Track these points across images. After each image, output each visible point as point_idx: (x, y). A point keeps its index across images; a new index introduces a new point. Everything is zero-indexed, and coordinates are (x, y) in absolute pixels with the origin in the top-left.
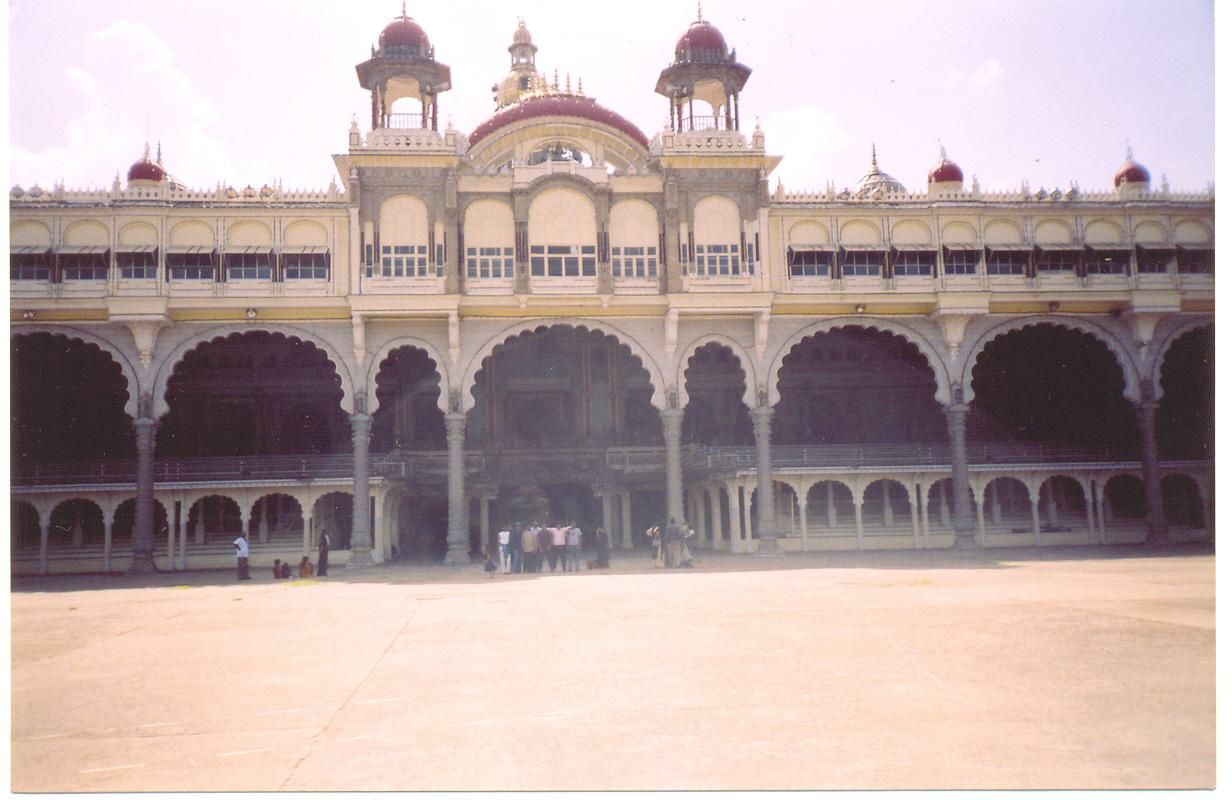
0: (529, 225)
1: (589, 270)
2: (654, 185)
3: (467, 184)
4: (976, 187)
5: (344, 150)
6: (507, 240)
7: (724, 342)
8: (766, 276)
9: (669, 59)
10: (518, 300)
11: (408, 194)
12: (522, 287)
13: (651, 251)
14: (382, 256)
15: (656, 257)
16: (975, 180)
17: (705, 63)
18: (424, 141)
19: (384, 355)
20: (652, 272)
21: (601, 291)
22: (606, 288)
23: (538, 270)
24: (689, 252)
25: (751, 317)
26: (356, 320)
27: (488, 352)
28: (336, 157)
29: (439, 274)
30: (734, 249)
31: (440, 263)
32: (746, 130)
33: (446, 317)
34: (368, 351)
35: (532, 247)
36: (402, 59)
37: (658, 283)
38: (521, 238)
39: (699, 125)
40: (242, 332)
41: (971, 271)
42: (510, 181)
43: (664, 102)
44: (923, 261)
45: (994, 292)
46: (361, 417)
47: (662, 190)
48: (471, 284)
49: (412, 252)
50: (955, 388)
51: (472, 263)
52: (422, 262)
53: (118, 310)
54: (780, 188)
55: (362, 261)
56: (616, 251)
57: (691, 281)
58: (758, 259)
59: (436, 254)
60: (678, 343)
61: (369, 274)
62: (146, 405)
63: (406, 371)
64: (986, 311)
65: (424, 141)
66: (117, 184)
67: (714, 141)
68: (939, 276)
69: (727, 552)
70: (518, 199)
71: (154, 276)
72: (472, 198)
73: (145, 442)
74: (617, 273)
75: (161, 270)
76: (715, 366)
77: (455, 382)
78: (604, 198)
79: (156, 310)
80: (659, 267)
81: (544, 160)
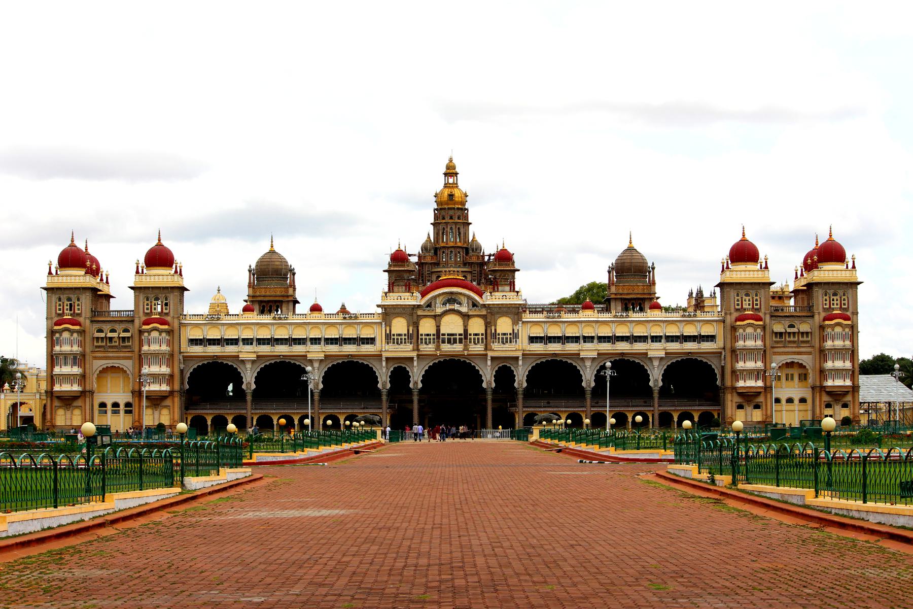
1: (461, 342)
2: (484, 312)
3: (420, 313)
5: (379, 303)
6: (433, 331)
22: (466, 348)
23: (443, 342)
24: (495, 335)
38: (438, 331)
41: (592, 342)
44: (576, 339)
53: (310, 356)
57: (496, 346)
59: (409, 336)
63: (400, 375)
75: (322, 342)
76: (505, 374)
77: (416, 379)
78: (466, 317)
79: (322, 356)
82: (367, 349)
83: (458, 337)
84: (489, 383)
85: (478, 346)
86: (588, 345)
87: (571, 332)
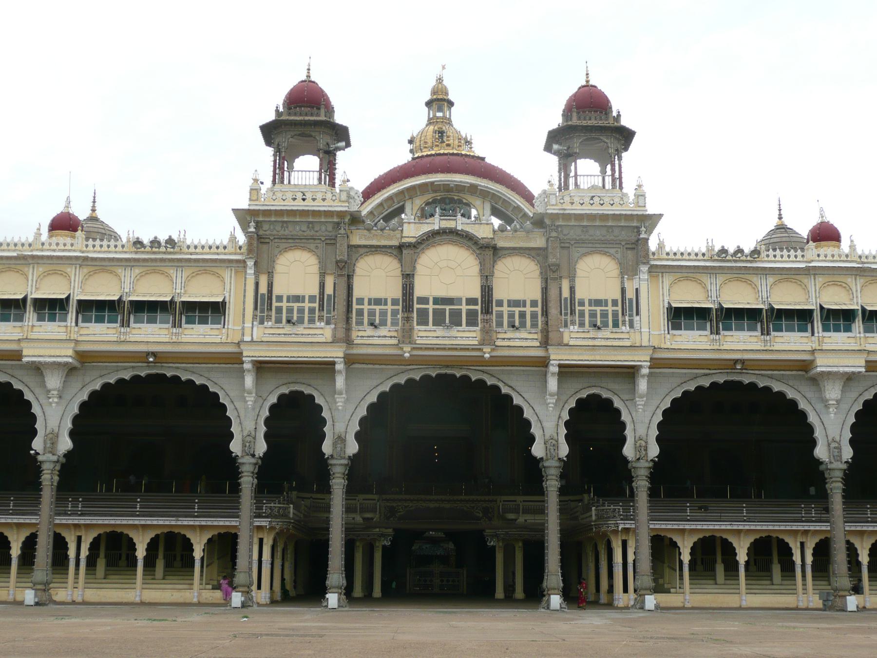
0: (416, 277)
1: (472, 320)
2: (539, 241)
3: (358, 238)
4: (852, 247)
5: (244, 204)
6: (393, 290)
7: (605, 395)
8: (645, 330)
9: (556, 121)
10: (402, 349)
11: (303, 248)
12: (407, 335)
13: (534, 303)
14: (275, 304)
15: (539, 309)
16: (852, 241)
17: (591, 126)
18: (319, 196)
19: (273, 399)
20: (534, 325)
21: (483, 342)
22: (487, 338)
23: (423, 321)
24: (571, 304)
25: (632, 370)
26: (247, 366)
27: (373, 398)
28: (235, 211)
29: (328, 323)
30: (615, 303)
31: (329, 312)
32: (629, 188)
33: (333, 364)
34: (258, 396)
35: (418, 298)
36: (305, 123)
37: (540, 335)
39: (584, 183)
40: (143, 374)
41: (848, 329)
42: (399, 236)
43: (553, 161)
45: (869, 352)
46: (248, 459)
47: (545, 246)
48: (354, 334)
49: (303, 302)
50: (833, 445)
51: (360, 313)
52: (312, 311)
53: (30, 354)
54: (661, 246)
55: (256, 308)
56: (500, 303)
57: (572, 334)
58: (637, 314)
60: (559, 393)
61: (262, 322)
62: (53, 439)
63: (295, 419)
64: (863, 370)
65: (319, 196)
66: (38, 234)
67: (596, 199)
68: (816, 334)
69: (610, 605)
70: (405, 252)
71: (65, 321)
72: (362, 251)
73: (49, 478)
74: (500, 324)
75: (72, 315)
77: (340, 428)
78: (488, 252)
79: (66, 354)
80: (540, 319)
81: (432, 215)
82: (198, 336)
83: (464, 308)
84: (551, 444)
85: (524, 335)
86: (837, 339)
87: (787, 298)
